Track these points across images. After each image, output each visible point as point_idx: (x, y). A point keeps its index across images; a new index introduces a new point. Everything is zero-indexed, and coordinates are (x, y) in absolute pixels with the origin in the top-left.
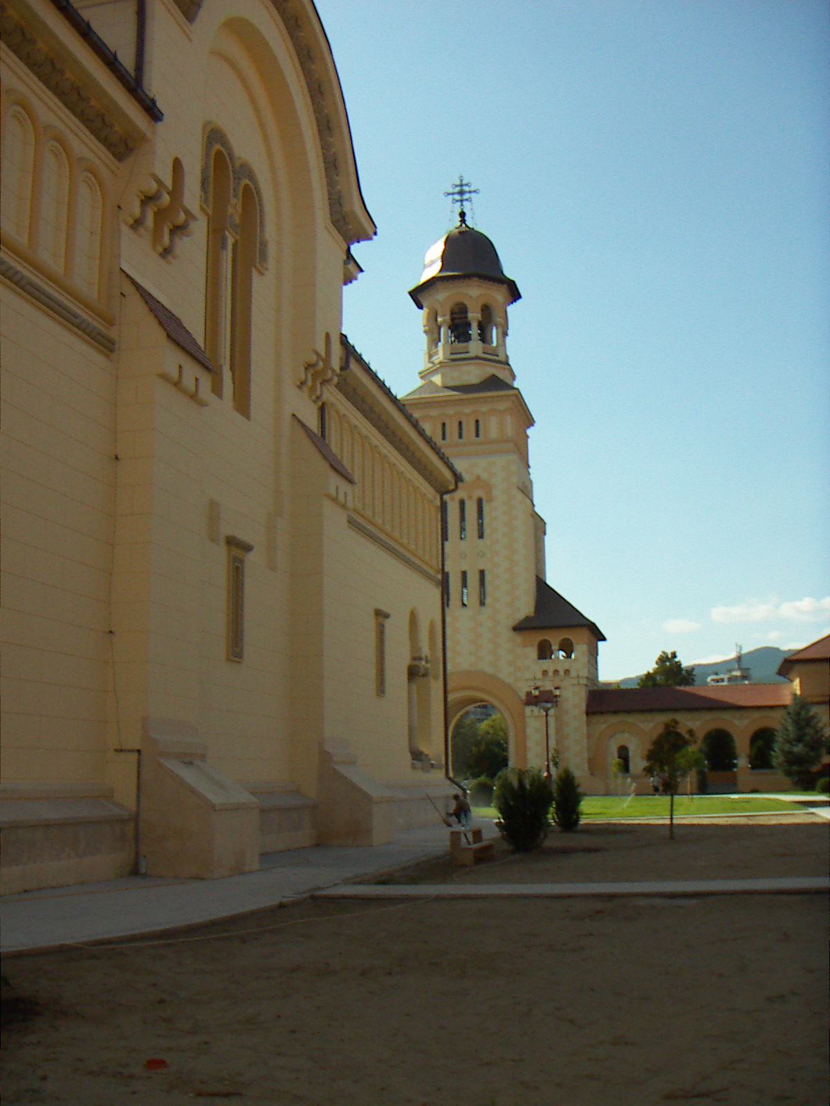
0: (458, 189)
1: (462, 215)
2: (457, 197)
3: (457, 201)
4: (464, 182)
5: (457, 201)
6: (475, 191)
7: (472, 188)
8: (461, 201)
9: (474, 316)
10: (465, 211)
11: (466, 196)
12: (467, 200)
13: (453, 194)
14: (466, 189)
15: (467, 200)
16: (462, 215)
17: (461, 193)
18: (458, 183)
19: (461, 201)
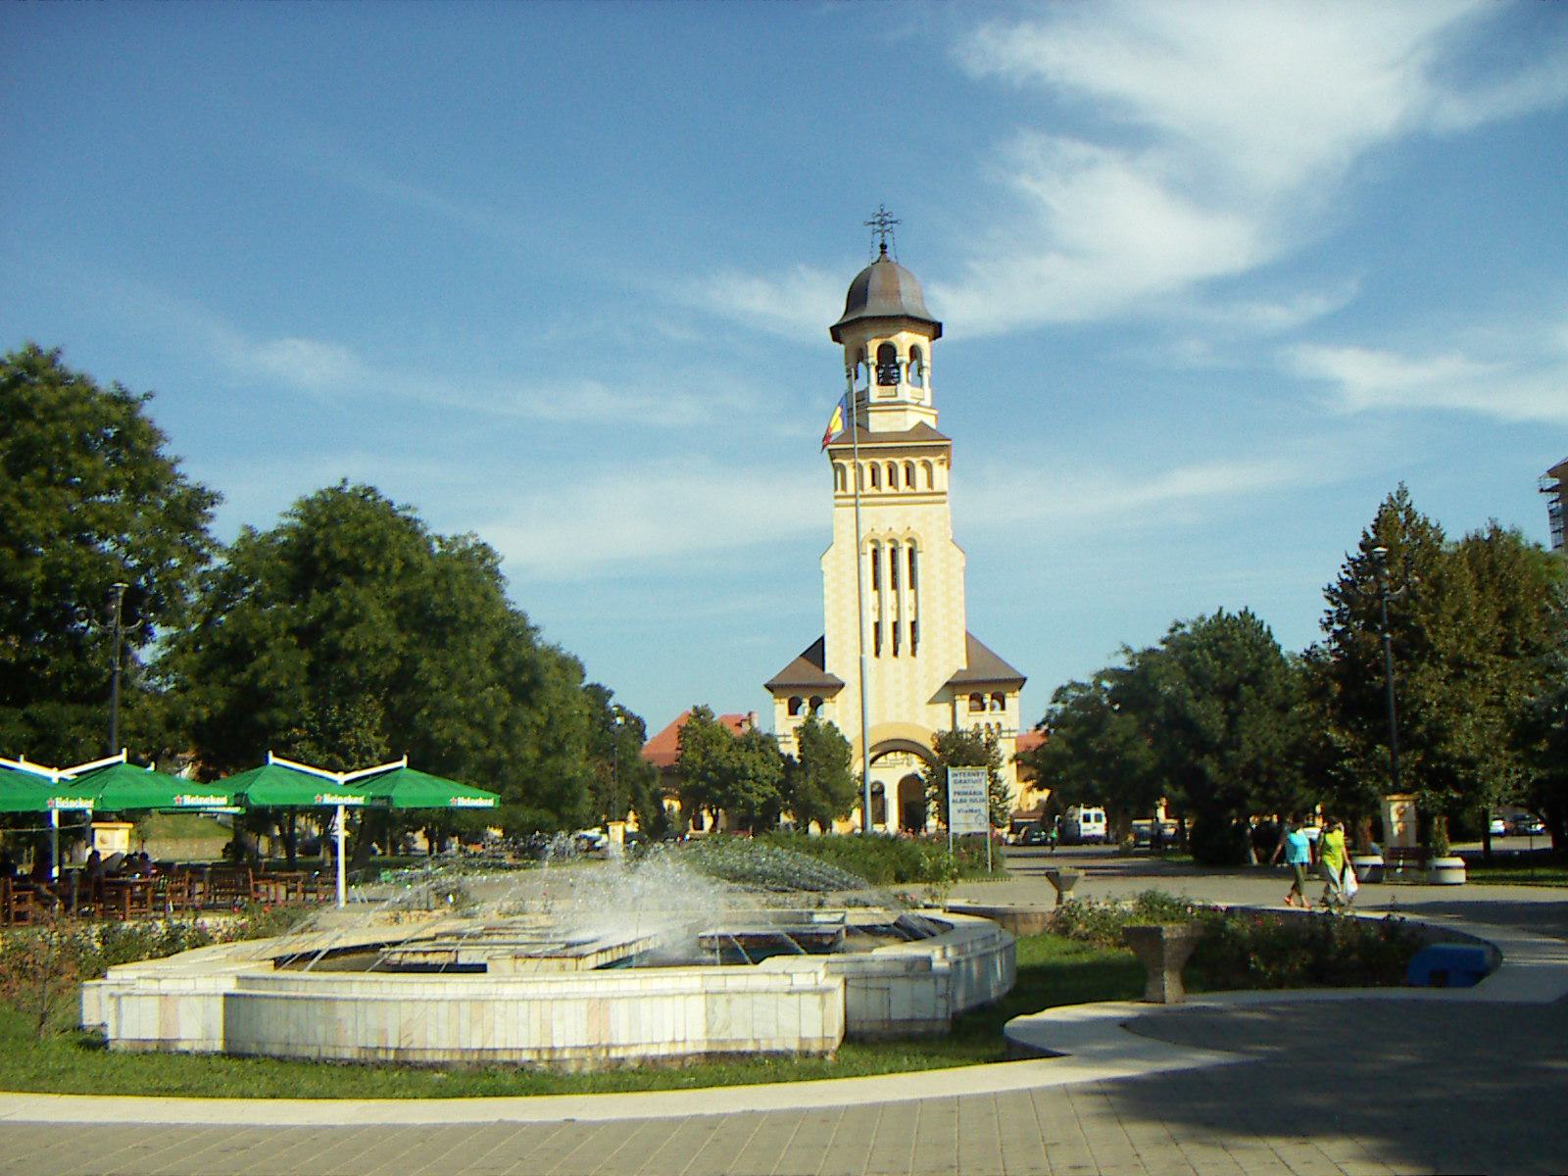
0: (877, 219)
1: (883, 247)
2: (877, 227)
3: (878, 231)
4: (886, 211)
5: (878, 231)
6: (896, 222)
7: (894, 219)
8: (883, 233)
9: (903, 356)
10: (886, 242)
11: (889, 226)
12: (888, 231)
13: (874, 223)
14: (887, 218)
15: (888, 231)
16: (883, 247)
17: (883, 223)
18: (879, 212)
19: (883, 233)
